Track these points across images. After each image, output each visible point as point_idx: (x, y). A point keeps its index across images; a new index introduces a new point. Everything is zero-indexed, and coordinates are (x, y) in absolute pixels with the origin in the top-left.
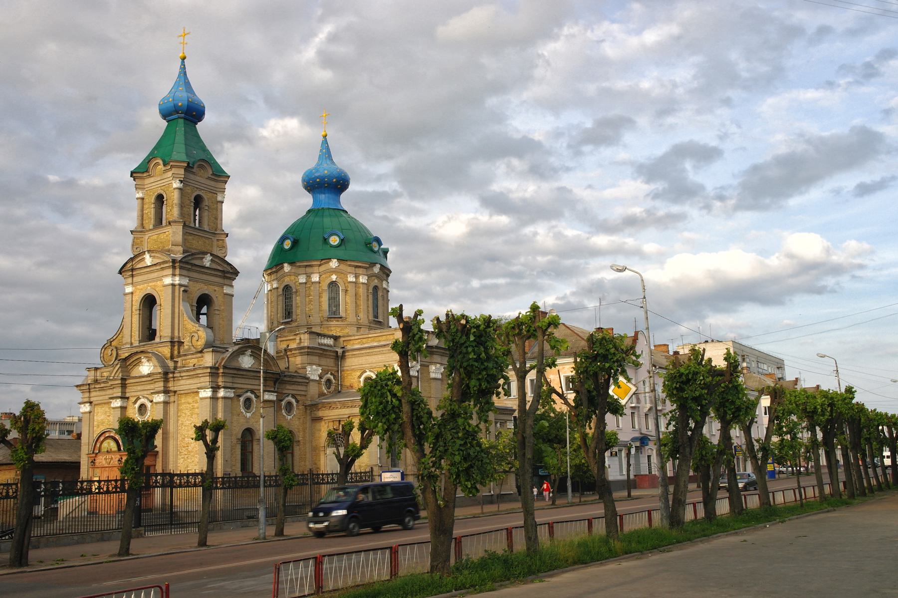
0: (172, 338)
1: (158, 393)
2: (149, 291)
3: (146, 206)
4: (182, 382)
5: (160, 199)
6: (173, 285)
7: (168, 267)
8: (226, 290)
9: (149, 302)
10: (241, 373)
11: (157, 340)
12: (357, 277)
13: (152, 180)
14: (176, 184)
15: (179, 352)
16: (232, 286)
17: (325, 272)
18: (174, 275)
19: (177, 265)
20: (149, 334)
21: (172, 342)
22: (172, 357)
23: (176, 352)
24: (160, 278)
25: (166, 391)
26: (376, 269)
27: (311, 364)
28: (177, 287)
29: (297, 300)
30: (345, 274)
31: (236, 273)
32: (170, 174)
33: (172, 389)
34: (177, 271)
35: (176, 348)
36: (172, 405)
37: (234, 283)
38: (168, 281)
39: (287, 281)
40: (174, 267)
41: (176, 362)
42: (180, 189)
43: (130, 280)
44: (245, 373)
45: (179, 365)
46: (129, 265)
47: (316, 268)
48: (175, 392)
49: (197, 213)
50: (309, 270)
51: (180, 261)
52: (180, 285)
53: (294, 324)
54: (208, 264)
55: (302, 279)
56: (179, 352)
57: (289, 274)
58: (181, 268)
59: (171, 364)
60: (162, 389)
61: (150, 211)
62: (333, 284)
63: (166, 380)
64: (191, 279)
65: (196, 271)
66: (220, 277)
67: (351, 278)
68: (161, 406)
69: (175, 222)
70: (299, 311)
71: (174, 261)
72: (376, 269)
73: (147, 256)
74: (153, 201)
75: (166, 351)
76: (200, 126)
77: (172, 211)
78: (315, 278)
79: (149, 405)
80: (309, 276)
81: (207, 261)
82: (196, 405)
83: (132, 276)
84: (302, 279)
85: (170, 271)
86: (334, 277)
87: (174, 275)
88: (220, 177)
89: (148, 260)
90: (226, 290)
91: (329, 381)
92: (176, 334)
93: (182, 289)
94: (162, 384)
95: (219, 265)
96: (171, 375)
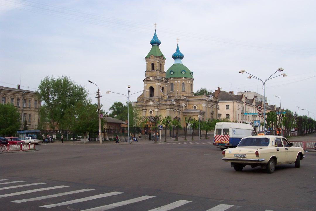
2: (151, 86)
5: (153, 64)
17: (181, 80)
20: (152, 95)
27: (183, 103)
29: (174, 87)
30: (186, 81)
32: (156, 59)
39: (172, 82)
47: (179, 79)
50: (178, 80)
53: (174, 93)
54: (163, 80)
55: (176, 82)
57: (172, 80)
61: (151, 67)
62: (183, 83)
64: (161, 84)
66: (164, 82)
67: (187, 82)
70: (175, 89)
76: (159, 46)
78: (179, 82)
79: (153, 111)
80: (178, 81)
82: (165, 112)
84: (176, 82)
86: (184, 82)
88: (165, 59)
91: (186, 107)
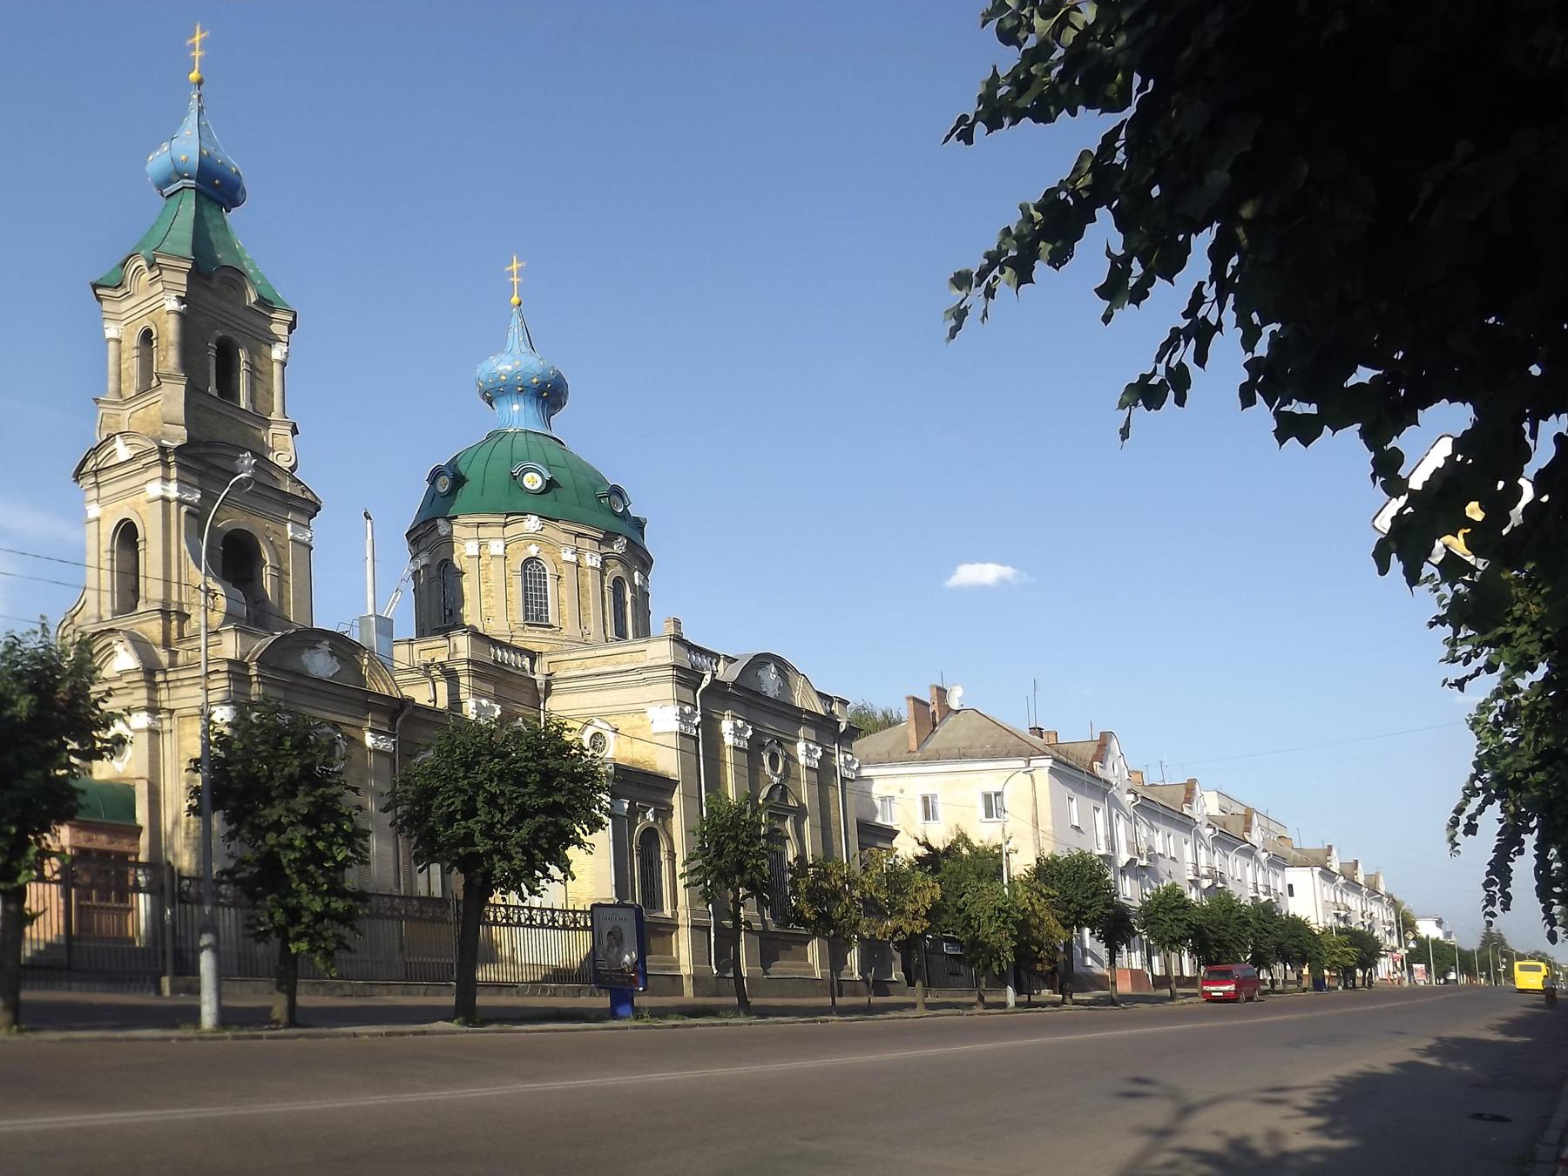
0: (166, 601)
1: (138, 709)
3: (124, 356)
4: (183, 692)
5: (147, 336)
6: (165, 500)
9: (127, 534)
10: (306, 683)
11: (141, 608)
14: (173, 305)
15: (181, 635)
18: (166, 479)
19: (171, 459)
20: (128, 595)
21: (165, 613)
22: (166, 643)
23: (174, 634)
24: (140, 489)
25: (153, 709)
28: (174, 505)
32: (159, 287)
33: (165, 705)
34: (174, 473)
35: (175, 623)
36: (167, 737)
38: (155, 489)
40: (166, 465)
41: (174, 654)
42: (178, 313)
43: (93, 494)
44: (314, 685)
45: (181, 659)
46: (90, 465)
48: (172, 711)
51: (179, 451)
52: (181, 502)
56: (181, 635)
58: (180, 467)
59: (164, 657)
60: (145, 703)
63: (153, 687)
68: (145, 737)
69: (169, 376)
71: (163, 450)
73: (119, 442)
74: (135, 341)
75: (153, 629)
77: (168, 358)
83: (97, 485)
85: (158, 471)
87: (166, 479)
89: (122, 451)
92: (175, 597)
93: (184, 509)
94: (143, 693)
96: (159, 678)
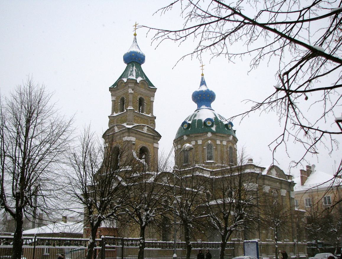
7: (126, 132)
8: (155, 145)
12: (221, 142)
13: (119, 91)
16: (158, 144)
26: (231, 138)
31: (160, 136)
37: (159, 142)
49: (141, 108)
65: (139, 134)
72: (231, 138)
76: (143, 66)
81: (145, 130)
86: (209, 142)
90: (155, 145)
95: (151, 132)
